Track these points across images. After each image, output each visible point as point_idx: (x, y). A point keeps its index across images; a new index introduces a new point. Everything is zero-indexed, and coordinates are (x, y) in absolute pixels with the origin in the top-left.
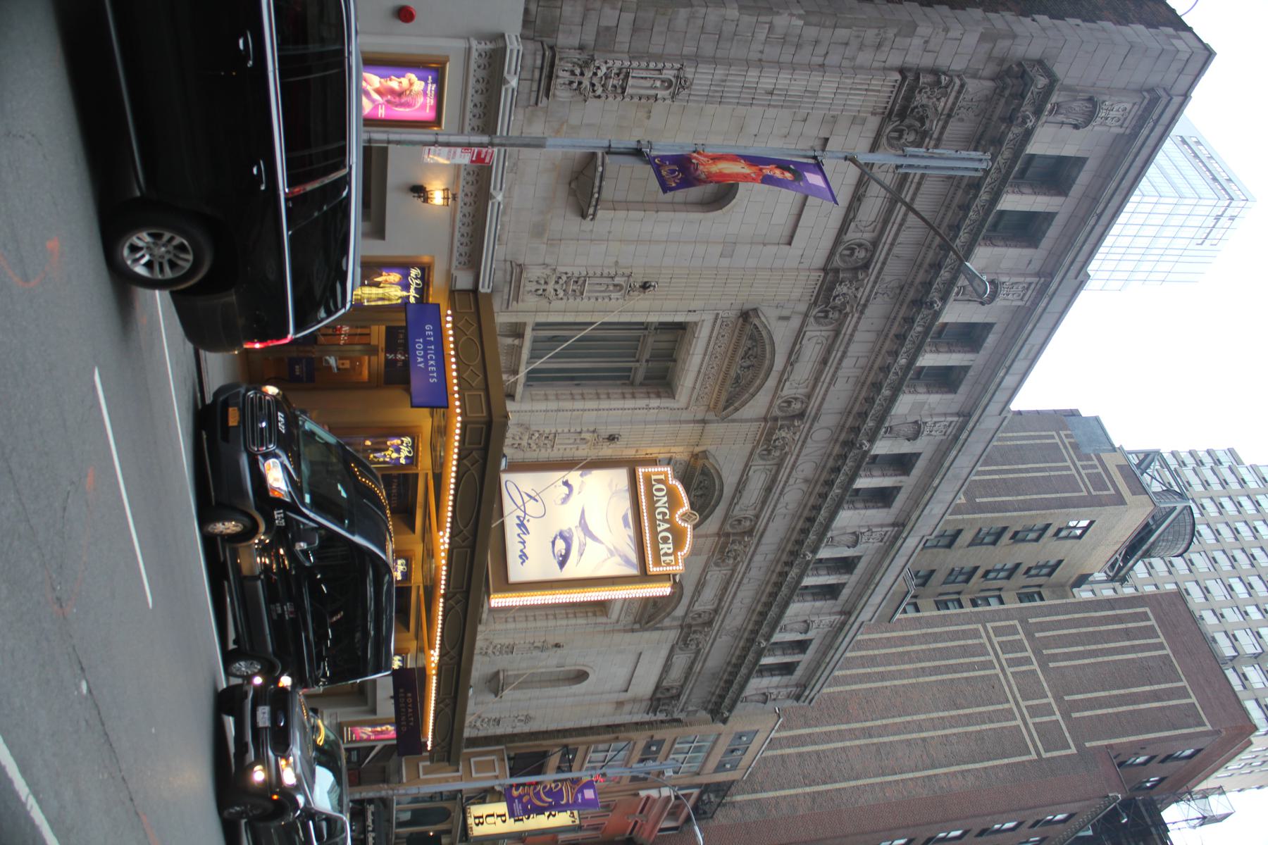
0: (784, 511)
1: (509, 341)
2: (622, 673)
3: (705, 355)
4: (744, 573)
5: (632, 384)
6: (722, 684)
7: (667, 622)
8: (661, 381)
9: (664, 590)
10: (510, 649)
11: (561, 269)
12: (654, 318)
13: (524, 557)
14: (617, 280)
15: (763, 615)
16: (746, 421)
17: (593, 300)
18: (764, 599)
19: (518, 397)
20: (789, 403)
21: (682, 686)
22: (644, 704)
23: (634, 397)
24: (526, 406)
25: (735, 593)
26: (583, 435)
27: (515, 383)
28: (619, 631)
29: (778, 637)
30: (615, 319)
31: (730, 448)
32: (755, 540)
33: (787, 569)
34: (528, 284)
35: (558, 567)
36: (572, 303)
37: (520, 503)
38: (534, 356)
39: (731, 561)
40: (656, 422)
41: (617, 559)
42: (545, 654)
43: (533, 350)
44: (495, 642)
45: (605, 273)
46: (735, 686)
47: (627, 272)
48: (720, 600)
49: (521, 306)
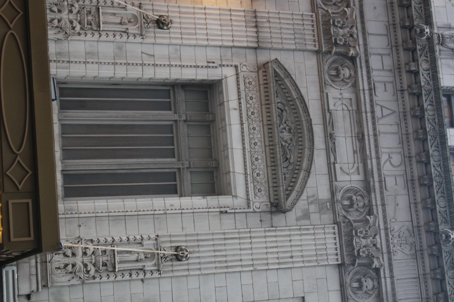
4: (370, 89)
25: (375, 135)
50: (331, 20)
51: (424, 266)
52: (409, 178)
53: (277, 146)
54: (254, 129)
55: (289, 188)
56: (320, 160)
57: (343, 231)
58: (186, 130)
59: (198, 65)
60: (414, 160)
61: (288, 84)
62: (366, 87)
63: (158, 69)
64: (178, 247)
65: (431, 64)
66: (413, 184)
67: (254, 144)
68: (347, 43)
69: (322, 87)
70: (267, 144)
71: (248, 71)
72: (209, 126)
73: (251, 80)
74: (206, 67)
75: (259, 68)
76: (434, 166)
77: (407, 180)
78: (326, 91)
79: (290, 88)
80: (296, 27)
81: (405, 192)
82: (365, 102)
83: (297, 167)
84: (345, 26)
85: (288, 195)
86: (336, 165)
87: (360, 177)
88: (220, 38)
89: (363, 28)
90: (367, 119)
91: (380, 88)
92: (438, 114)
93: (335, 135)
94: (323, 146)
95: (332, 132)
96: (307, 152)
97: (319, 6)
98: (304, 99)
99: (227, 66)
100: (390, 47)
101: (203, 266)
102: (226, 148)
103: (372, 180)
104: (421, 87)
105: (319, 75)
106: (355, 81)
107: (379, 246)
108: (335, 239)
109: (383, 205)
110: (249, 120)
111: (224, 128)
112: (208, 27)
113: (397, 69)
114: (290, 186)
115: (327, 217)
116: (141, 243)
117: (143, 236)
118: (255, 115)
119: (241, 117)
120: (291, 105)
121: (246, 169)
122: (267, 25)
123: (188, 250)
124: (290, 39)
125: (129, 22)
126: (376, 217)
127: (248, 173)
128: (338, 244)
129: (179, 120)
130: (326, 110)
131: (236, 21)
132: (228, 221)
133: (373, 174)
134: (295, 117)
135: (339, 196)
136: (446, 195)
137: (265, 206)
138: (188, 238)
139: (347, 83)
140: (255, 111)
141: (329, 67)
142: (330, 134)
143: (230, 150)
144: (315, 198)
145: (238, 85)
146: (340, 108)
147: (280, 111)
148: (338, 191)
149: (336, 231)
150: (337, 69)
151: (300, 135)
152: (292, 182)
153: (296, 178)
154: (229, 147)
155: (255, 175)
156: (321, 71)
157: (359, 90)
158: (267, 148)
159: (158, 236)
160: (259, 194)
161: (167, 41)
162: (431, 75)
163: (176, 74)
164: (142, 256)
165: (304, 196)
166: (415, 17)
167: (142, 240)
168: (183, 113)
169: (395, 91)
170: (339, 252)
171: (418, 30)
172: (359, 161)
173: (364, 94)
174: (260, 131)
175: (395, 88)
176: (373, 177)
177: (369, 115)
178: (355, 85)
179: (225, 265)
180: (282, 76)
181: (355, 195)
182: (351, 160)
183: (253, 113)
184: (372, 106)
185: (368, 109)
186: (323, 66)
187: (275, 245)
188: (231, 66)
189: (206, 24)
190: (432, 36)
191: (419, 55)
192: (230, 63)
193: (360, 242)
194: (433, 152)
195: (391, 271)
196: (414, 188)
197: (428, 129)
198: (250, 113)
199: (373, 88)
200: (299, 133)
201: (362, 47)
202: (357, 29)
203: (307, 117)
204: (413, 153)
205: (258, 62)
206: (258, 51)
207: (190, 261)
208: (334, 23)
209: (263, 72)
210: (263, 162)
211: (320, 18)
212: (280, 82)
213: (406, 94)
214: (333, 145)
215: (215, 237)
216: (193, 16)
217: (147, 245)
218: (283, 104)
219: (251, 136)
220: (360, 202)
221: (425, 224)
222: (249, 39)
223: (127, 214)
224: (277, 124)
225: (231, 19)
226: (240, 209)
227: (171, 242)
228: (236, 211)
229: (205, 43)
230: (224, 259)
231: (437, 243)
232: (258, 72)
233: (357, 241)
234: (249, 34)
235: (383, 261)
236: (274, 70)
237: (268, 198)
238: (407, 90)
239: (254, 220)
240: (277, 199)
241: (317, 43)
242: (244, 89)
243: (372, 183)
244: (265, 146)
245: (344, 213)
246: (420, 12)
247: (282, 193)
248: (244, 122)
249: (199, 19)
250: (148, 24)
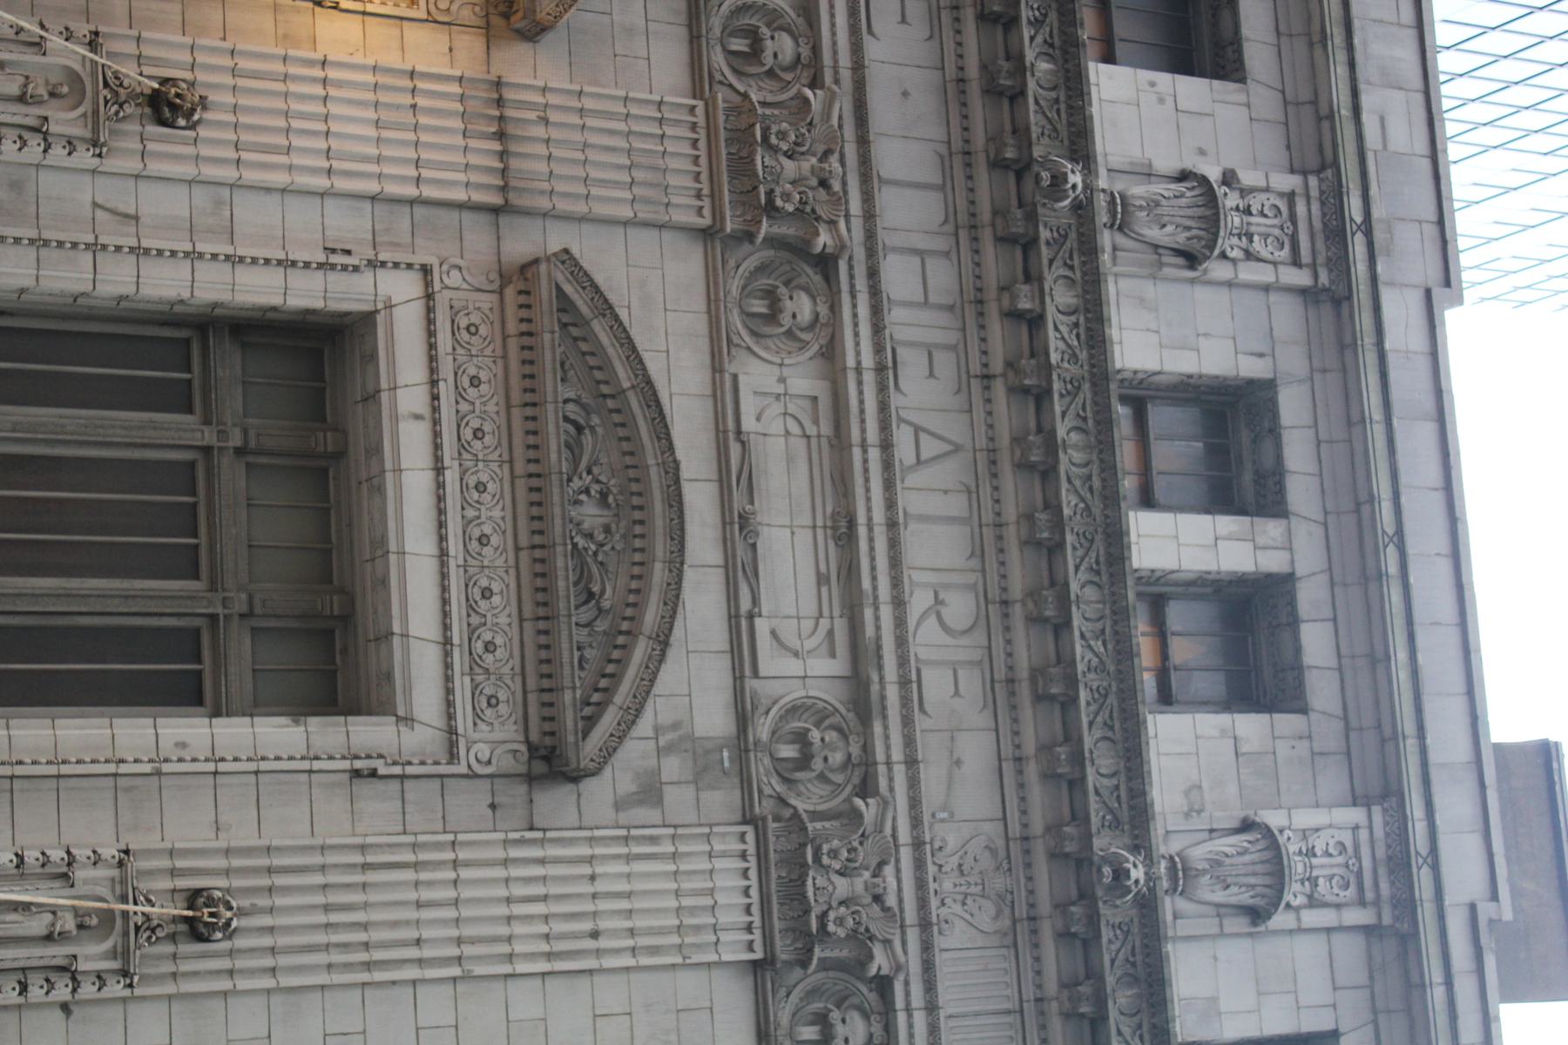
4: (880, 369)
25: (892, 525)
46: (1121, 999)
50: (758, 126)
51: (1039, 973)
52: (1000, 674)
53: (559, 549)
54: (481, 487)
55: (596, 697)
56: (703, 602)
57: (771, 848)
58: (243, 484)
59: (291, 257)
60: (1017, 611)
61: (605, 340)
62: (868, 360)
63: (151, 268)
64: (197, 892)
65: (1086, 292)
66: (1012, 694)
67: (479, 540)
68: (808, 209)
69: (720, 352)
70: (524, 540)
71: (465, 286)
72: (325, 471)
73: (475, 319)
74: (320, 266)
75: (505, 279)
76: (1083, 636)
77: (993, 681)
78: (731, 368)
79: (610, 351)
80: (638, 144)
81: (985, 720)
82: (862, 411)
83: (625, 626)
84: (804, 149)
85: (591, 722)
86: (757, 621)
87: (837, 666)
88: (374, 168)
89: (865, 161)
90: (866, 470)
91: (912, 367)
92: (1102, 461)
93: (759, 519)
94: (714, 556)
95: (748, 507)
96: (659, 573)
97: (718, 77)
98: (655, 394)
99: (396, 265)
100: (950, 228)
101: (283, 961)
102: (379, 553)
103: (875, 677)
105: (709, 311)
106: (833, 336)
107: (891, 901)
108: (745, 873)
109: (911, 762)
110: (465, 455)
111: (375, 482)
112: (335, 127)
113: (972, 304)
114: (597, 690)
115: (722, 800)
116: (65, 876)
117: (74, 851)
118: (487, 439)
119: (437, 446)
120: (611, 411)
121: (446, 627)
122: (539, 131)
123: (234, 904)
124: (616, 184)
125: (52, 94)
126: (886, 803)
127: (456, 640)
128: (754, 892)
129: (220, 448)
130: (728, 434)
131: (431, 112)
132: (378, 806)
133: (880, 657)
134: (624, 454)
135: (762, 729)
136: (1118, 736)
137: (510, 756)
138: (237, 862)
139: (804, 345)
140: (487, 428)
141: (744, 288)
142: (740, 516)
143: (393, 558)
144: (681, 732)
145: (431, 334)
146: (777, 427)
147: (571, 429)
148: (762, 710)
149: (751, 848)
150: (771, 295)
151: (637, 515)
152: (604, 676)
153: (618, 661)
154: (393, 547)
155: (479, 647)
156: (717, 300)
157: (845, 369)
158: (524, 555)
159: (127, 852)
160: (489, 712)
161: (188, 170)
162: (1082, 330)
163: (212, 287)
164: (69, 923)
165: (644, 726)
166: (1035, 131)
167: (69, 864)
168: (234, 425)
169: (964, 376)
170: (756, 919)
171: (1045, 175)
172: (836, 612)
173: (860, 383)
174: (502, 496)
175: (963, 369)
176: (880, 668)
177: (874, 454)
178: (830, 353)
179: (363, 956)
180: (584, 310)
181: (817, 725)
182: (809, 606)
183: (478, 434)
184: (885, 426)
185: (873, 435)
186: (725, 283)
187: (539, 890)
188: (410, 266)
189: (326, 119)
190: (1090, 200)
191: (1045, 262)
192: (403, 257)
193: (830, 888)
194: (1083, 587)
195: (930, 986)
196: (1014, 707)
197: (1067, 512)
198: (467, 434)
199: (890, 364)
200: (634, 508)
201: (857, 224)
202: (843, 164)
203: (663, 453)
204: (1017, 589)
205: (503, 259)
206: (504, 220)
207: (240, 942)
208: (765, 138)
209: (520, 292)
210: (508, 603)
211: (721, 118)
212: (575, 332)
213: (999, 388)
214: (750, 554)
215: (332, 859)
216: (279, 87)
217: (85, 882)
218: (583, 407)
219: (470, 513)
220: (834, 750)
221: (1048, 829)
222: (475, 178)
223: (19, 770)
224: (561, 473)
225: (414, 106)
226: (423, 763)
227: (173, 873)
228: (409, 770)
229: (322, 183)
230: (362, 937)
231: (1086, 895)
232: (501, 293)
233: (820, 882)
234: (473, 159)
235: (905, 952)
236: (559, 288)
237: (521, 728)
238: (1004, 375)
239: (469, 803)
240: (552, 734)
241: (706, 203)
242: (450, 350)
243: (875, 688)
244: (517, 549)
245: (778, 789)
246: (1053, 115)
247: (569, 714)
248: (447, 462)
249: (302, 97)
250: (121, 106)
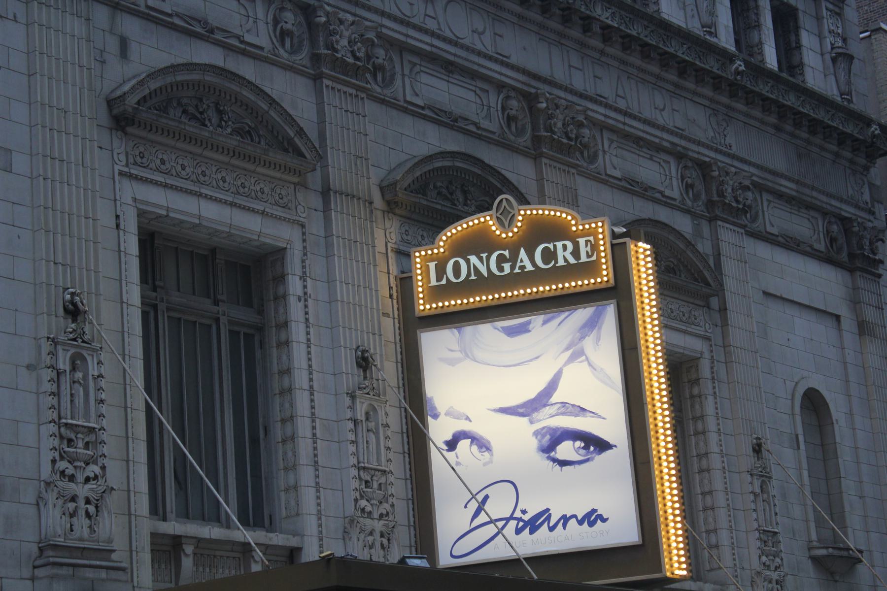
0: (487, 38)
1: (187, 563)
2: (805, 327)
3: (200, 195)
4: (607, 106)
5: (260, 329)
6: (817, 140)
7: (705, 247)
8: (253, 275)
9: (641, 254)
10: (768, 537)
11: (46, 471)
12: (134, 294)
13: (592, 518)
14: (64, 364)
15: (683, 68)
16: (321, 113)
17: (104, 409)
18: (655, 69)
19: (293, 542)
20: (284, 34)
21: (825, 214)
22: (861, 283)
23: (285, 325)
24: (310, 524)
25: (646, 122)
26: (360, 416)
27: (266, 548)
28: (724, 335)
29: (726, 39)
30: (139, 365)
31: (373, 143)
32: (544, 88)
33: (596, 28)
34: (77, 533)
35: (609, 452)
36: (111, 447)
37: (491, 530)
38: (216, 517)
39: (586, 132)
40: (330, 281)
41: (588, 344)
42: (776, 472)
43: (203, 518)
44: (756, 565)
45: (48, 387)
46: (821, 115)
47: (46, 346)
48: (659, 149)
49: (120, 544)
52: (672, 88)
62: (601, 110)
103: (679, 148)
104: (618, 28)
132: (723, 374)
176: (677, 145)
177: (628, 121)
